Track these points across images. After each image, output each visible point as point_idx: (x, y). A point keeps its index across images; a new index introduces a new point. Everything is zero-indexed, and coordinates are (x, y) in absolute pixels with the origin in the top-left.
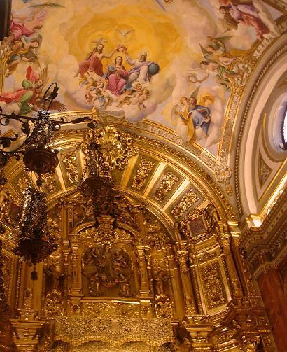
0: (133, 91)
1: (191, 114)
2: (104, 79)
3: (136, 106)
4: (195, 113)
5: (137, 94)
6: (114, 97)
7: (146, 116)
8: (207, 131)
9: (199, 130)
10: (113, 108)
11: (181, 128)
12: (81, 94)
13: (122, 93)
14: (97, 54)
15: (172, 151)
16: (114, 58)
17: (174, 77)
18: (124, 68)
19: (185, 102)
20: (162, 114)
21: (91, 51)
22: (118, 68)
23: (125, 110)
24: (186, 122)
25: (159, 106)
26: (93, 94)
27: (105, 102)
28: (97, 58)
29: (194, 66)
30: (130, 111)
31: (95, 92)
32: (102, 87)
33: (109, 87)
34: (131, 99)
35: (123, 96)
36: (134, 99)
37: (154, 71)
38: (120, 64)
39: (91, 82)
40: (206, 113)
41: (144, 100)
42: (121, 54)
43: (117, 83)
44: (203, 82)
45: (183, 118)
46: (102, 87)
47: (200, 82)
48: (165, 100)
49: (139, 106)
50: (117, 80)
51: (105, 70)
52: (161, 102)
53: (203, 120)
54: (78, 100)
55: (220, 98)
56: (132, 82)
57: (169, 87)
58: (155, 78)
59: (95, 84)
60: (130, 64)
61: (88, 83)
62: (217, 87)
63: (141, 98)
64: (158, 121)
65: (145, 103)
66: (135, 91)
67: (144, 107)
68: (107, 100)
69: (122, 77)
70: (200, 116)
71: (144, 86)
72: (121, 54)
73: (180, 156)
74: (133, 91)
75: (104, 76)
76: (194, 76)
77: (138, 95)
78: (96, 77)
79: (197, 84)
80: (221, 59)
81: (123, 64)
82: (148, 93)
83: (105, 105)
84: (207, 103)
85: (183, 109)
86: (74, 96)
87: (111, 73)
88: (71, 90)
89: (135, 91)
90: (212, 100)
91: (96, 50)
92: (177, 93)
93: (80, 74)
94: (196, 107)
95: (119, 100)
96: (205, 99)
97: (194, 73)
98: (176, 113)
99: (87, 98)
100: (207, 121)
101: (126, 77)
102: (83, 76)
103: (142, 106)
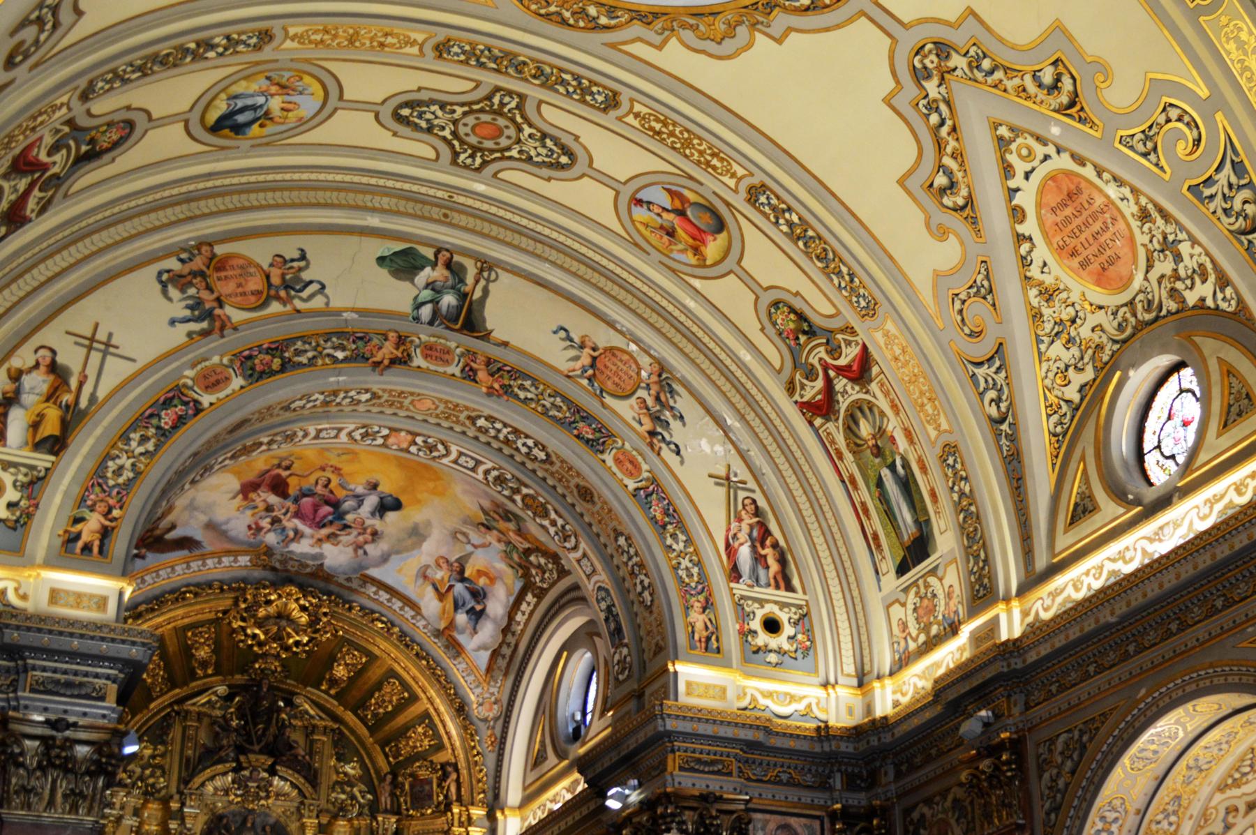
0: (346, 527)
1: (451, 587)
2: (289, 503)
3: (350, 550)
4: (459, 588)
5: (355, 533)
6: (307, 530)
7: (367, 568)
8: (476, 622)
9: (462, 618)
10: (302, 547)
11: (430, 604)
12: (238, 521)
13: (324, 526)
14: (280, 471)
15: (406, 641)
16: (312, 479)
17: (428, 524)
18: (331, 492)
19: (445, 566)
20: (400, 571)
21: (268, 467)
22: (319, 489)
23: (326, 553)
24: (441, 596)
25: (394, 558)
26: (265, 523)
27: (287, 536)
28: (279, 476)
29: (464, 523)
30: (336, 556)
31: (268, 520)
32: (285, 514)
33: (297, 515)
34: (341, 538)
35: (325, 532)
36: (344, 538)
37: (388, 505)
38: (326, 486)
39: (262, 506)
40: (478, 595)
41: (366, 542)
42: (328, 474)
43: (316, 511)
44: (480, 550)
45: (436, 589)
46: (285, 514)
47: (475, 547)
48: (407, 550)
49: (355, 551)
50: (316, 508)
51: (292, 491)
52: (398, 552)
53: (471, 603)
54: (233, 533)
55: (505, 584)
56: (347, 512)
57: (417, 535)
58: (391, 516)
59: (269, 509)
60: (344, 488)
61: (256, 507)
62: (501, 566)
63: (361, 538)
64: (389, 581)
65: (368, 548)
66: (350, 527)
67: (365, 553)
68: (291, 534)
69: (327, 502)
70: (467, 596)
71: (369, 522)
72: (328, 474)
73: (422, 655)
74: (346, 527)
75: (292, 498)
76: (464, 534)
77: (355, 533)
78: (273, 499)
79: (469, 548)
80: (511, 534)
81: (332, 486)
82: (375, 534)
83: (287, 541)
84: (482, 581)
85: (439, 575)
86: (224, 527)
87: (305, 495)
88: (220, 515)
89: (350, 527)
90: (492, 580)
91: (279, 466)
92: (430, 549)
93: (240, 496)
94: (463, 579)
95: (319, 536)
96: (480, 573)
97: (464, 530)
98: (425, 577)
99: (250, 527)
100: (478, 608)
101: (336, 504)
102: (246, 498)
103: (360, 552)
